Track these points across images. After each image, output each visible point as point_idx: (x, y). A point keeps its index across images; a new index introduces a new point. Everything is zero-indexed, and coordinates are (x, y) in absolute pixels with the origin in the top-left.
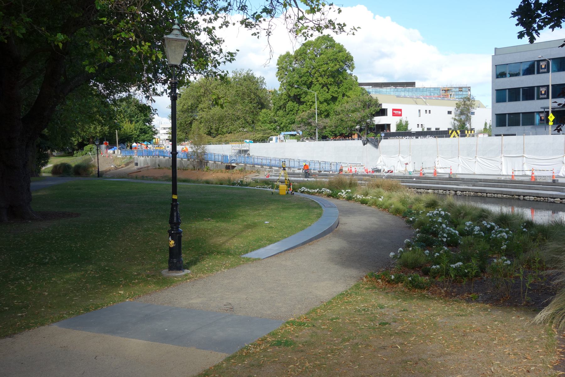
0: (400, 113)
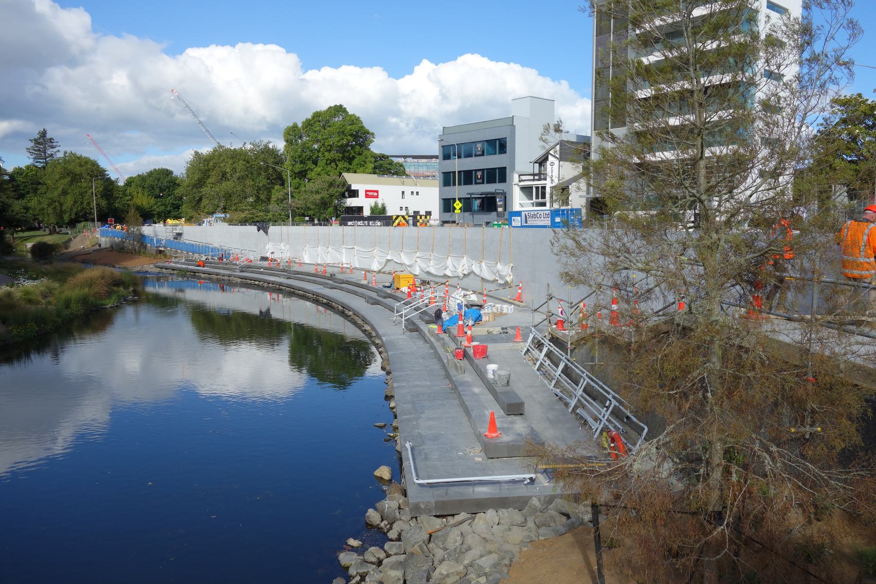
0: (375, 194)
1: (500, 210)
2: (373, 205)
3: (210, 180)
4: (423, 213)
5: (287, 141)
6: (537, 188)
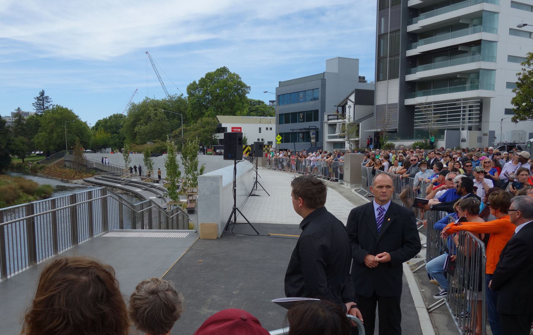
1: (313, 141)
4: (266, 143)
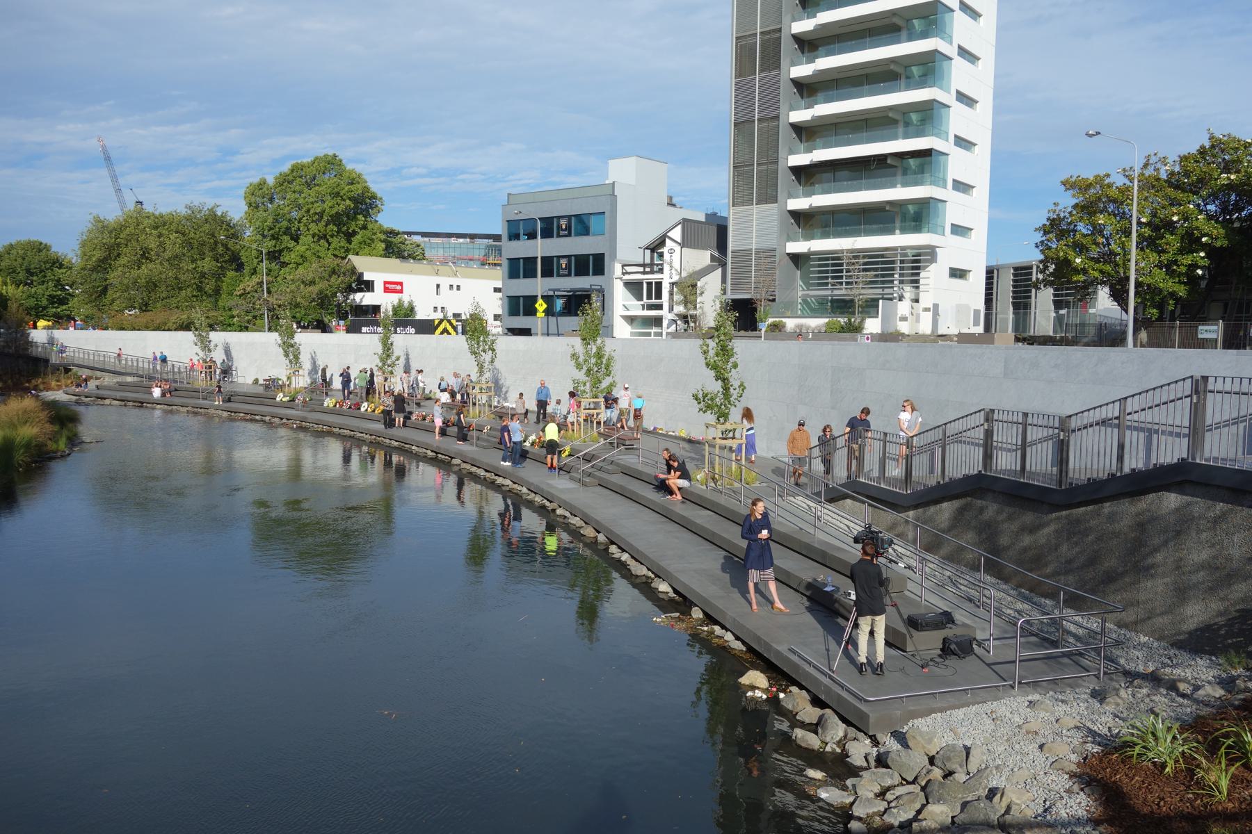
0: (399, 287)
2: (396, 302)
3: (123, 260)
5: (250, 205)
6: (649, 284)
